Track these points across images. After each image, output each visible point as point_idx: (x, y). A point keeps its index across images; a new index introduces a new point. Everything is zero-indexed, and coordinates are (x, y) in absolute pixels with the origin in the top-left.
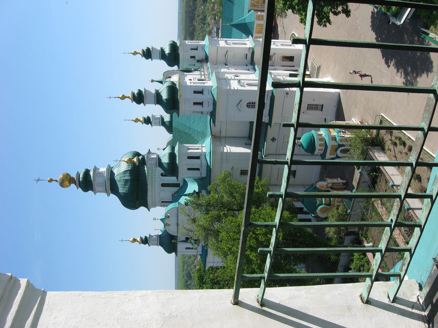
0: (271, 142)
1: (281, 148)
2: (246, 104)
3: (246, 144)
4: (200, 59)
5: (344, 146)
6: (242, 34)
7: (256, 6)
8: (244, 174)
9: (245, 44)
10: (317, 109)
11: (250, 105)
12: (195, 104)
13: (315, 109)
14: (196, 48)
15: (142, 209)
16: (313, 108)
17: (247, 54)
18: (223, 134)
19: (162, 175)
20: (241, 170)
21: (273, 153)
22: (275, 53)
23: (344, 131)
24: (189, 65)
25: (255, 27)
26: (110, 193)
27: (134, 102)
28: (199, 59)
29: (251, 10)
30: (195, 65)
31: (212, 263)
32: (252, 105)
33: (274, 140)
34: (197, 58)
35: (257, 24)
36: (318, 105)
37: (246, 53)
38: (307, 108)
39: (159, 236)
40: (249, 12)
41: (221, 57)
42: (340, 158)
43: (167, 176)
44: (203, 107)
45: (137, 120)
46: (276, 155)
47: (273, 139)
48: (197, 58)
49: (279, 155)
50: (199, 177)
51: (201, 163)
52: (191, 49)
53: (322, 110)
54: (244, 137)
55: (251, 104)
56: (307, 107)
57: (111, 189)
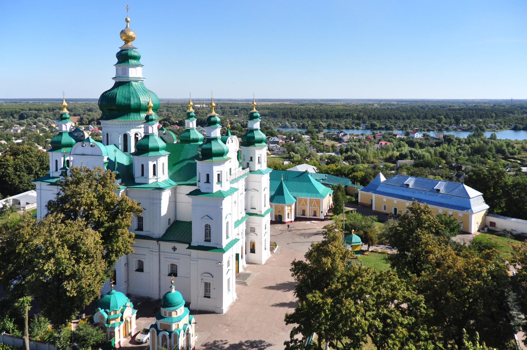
0: (172, 247)
2: (209, 224)
3: (169, 220)
4: (250, 165)
5: (170, 339)
6: (274, 190)
7: (299, 204)
8: (138, 219)
9: (265, 206)
14: (260, 162)
17: (255, 209)
20: (142, 217)
21: (161, 248)
25: (281, 204)
29: (296, 199)
31: (40, 187)
34: (250, 163)
40: (294, 197)
41: (252, 186)
46: (159, 252)
47: (175, 248)
48: (250, 163)
49: (159, 255)
52: (259, 157)
54: (176, 216)
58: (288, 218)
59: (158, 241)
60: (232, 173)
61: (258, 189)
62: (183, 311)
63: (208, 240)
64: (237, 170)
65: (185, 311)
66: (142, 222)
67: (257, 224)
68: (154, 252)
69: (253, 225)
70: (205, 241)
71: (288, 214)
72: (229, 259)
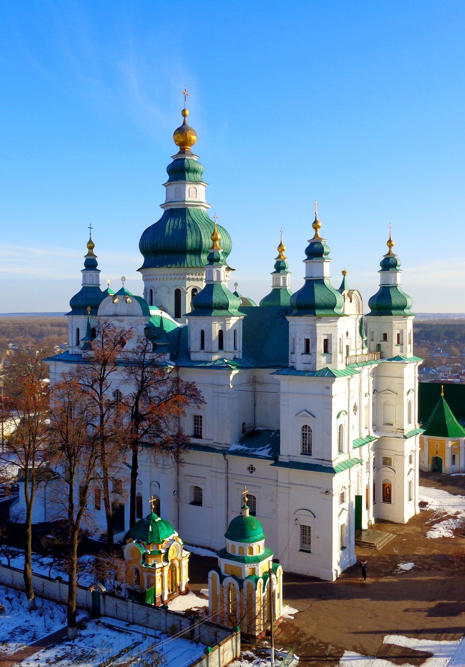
0: (248, 465)
1: (238, 482)
2: (308, 425)
3: (244, 424)
4: (382, 349)
5: (240, 590)
8: (195, 421)
10: (304, 543)
11: (306, 431)
12: (307, 341)
13: (304, 538)
15: (140, 260)
16: (304, 536)
17: (392, 425)
18: (258, 388)
19: (194, 290)
20: (201, 417)
21: (229, 468)
22: (395, 472)
23: (266, 589)
24: (373, 332)
26: (165, 208)
27: (309, 243)
28: (382, 347)
30: (372, 340)
32: (306, 434)
33: (250, 470)
34: (383, 344)
35: (445, 441)
36: (310, 544)
37: (394, 425)
38: (304, 526)
39: (96, 286)
41: (386, 383)
42: (220, 583)
43: (192, 298)
44: (302, 354)
45: (91, 245)
46: (227, 473)
47: (252, 469)
48: (383, 344)
49: (227, 478)
50: (190, 349)
51: (212, 352)
52: (398, 335)
53: (301, 550)
55: (308, 433)
56: (305, 526)
57: (171, 210)
58: (453, 462)
59: (224, 454)
60: (352, 353)
61: (396, 390)
62: (262, 552)
63: (307, 451)
64: (359, 352)
65: (265, 551)
66: (201, 425)
67: (395, 453)
68: (219, 473)
69: (387, 454)
70: (301, 454)
71: (454, 457)
72: (344, 490)
